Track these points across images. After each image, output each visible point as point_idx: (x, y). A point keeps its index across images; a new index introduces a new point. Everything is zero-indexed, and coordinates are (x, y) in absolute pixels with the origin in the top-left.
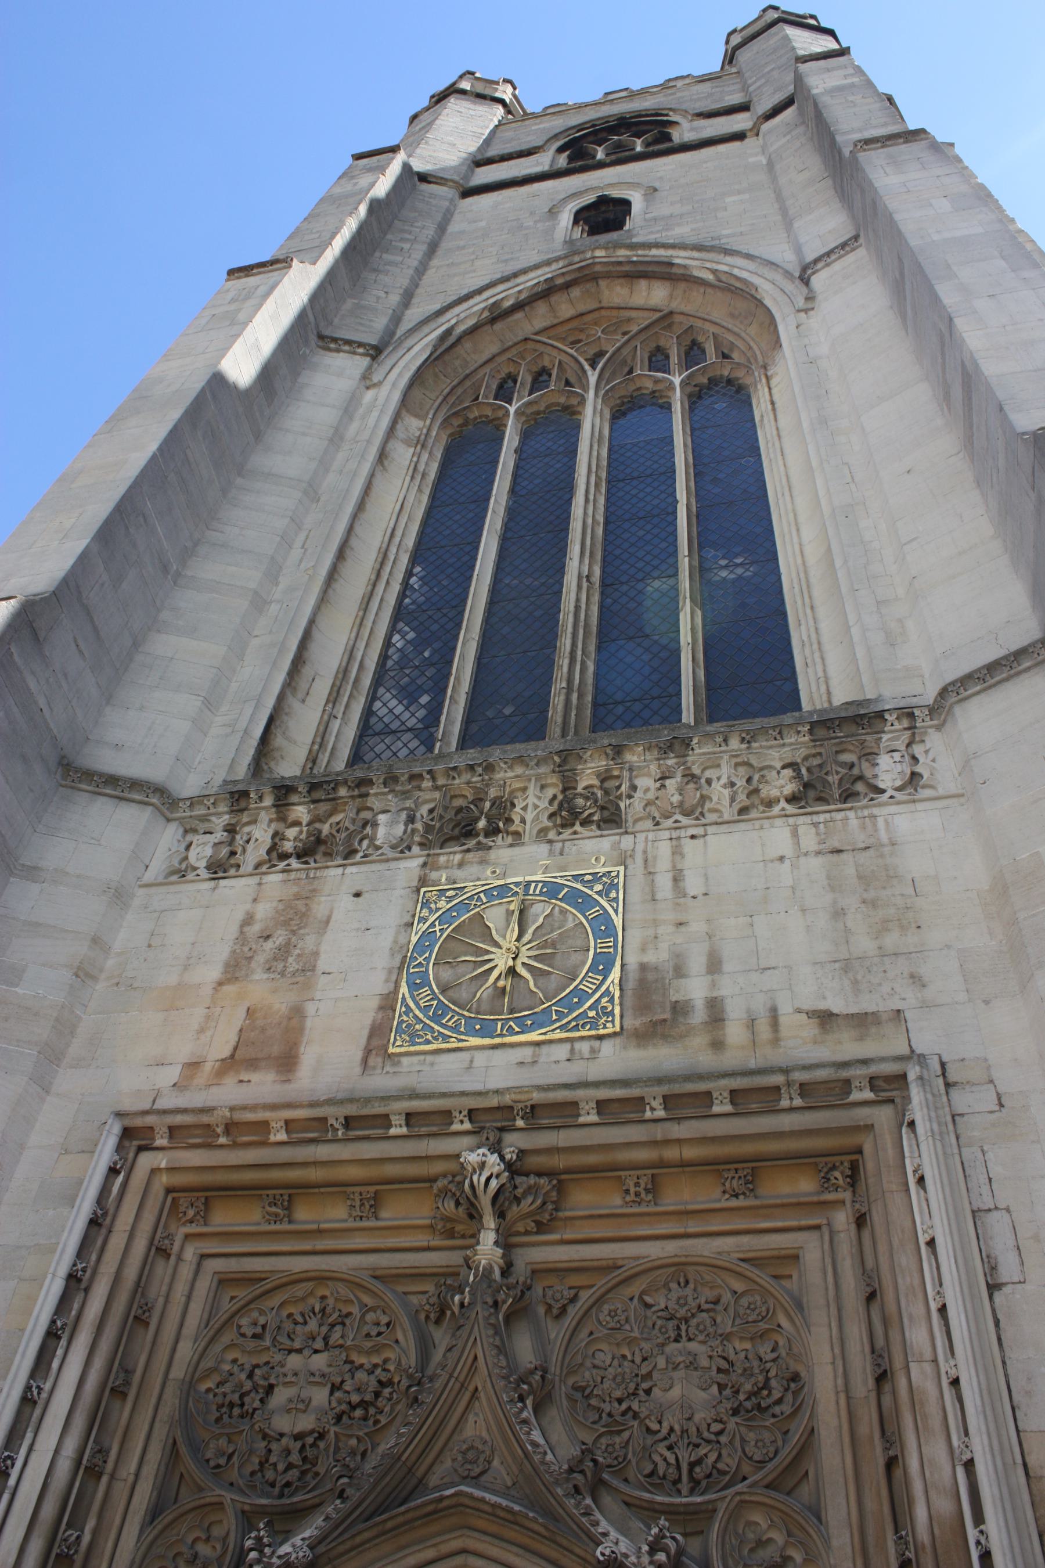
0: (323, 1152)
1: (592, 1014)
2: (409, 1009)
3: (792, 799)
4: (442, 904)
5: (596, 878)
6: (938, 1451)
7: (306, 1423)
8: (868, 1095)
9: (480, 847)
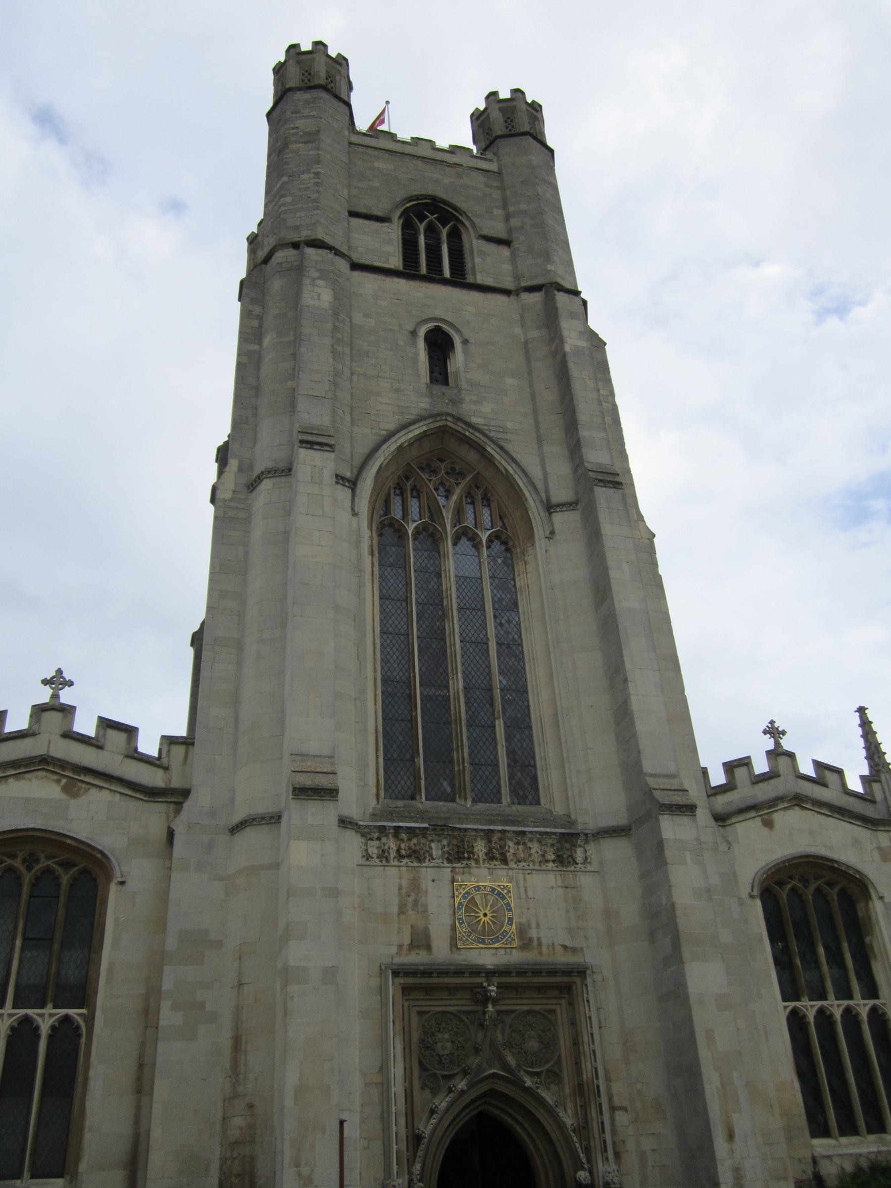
0: (447, 980)
1: (510, 939)
2: (460, 933)
3: (554, 861)
4: (462, 891)
5: (504, 887)
6: (589, 1064)
7: (447, 1052)
8: (576, 974)
9: (468, 866)
